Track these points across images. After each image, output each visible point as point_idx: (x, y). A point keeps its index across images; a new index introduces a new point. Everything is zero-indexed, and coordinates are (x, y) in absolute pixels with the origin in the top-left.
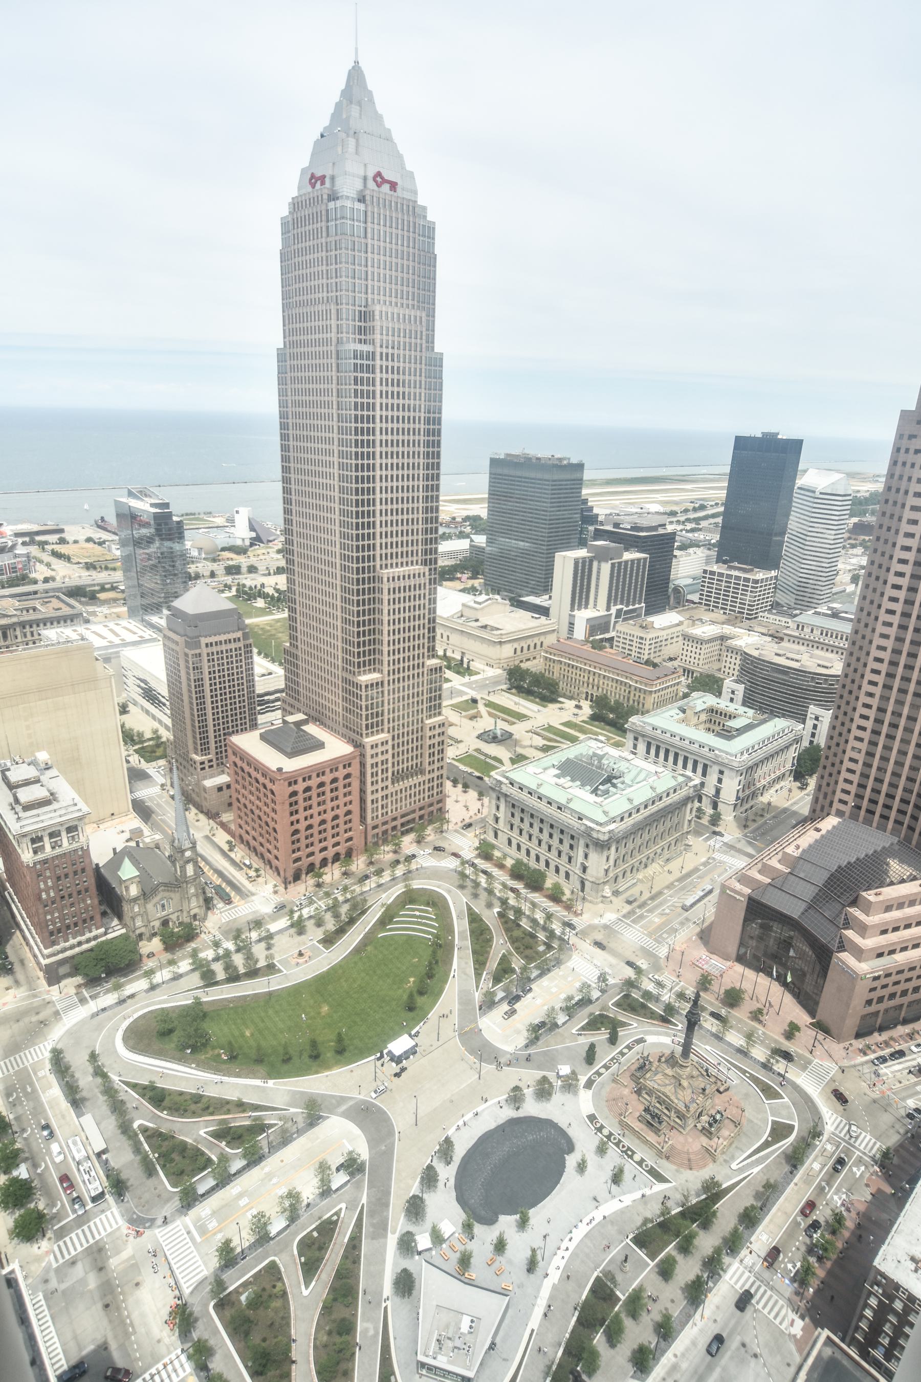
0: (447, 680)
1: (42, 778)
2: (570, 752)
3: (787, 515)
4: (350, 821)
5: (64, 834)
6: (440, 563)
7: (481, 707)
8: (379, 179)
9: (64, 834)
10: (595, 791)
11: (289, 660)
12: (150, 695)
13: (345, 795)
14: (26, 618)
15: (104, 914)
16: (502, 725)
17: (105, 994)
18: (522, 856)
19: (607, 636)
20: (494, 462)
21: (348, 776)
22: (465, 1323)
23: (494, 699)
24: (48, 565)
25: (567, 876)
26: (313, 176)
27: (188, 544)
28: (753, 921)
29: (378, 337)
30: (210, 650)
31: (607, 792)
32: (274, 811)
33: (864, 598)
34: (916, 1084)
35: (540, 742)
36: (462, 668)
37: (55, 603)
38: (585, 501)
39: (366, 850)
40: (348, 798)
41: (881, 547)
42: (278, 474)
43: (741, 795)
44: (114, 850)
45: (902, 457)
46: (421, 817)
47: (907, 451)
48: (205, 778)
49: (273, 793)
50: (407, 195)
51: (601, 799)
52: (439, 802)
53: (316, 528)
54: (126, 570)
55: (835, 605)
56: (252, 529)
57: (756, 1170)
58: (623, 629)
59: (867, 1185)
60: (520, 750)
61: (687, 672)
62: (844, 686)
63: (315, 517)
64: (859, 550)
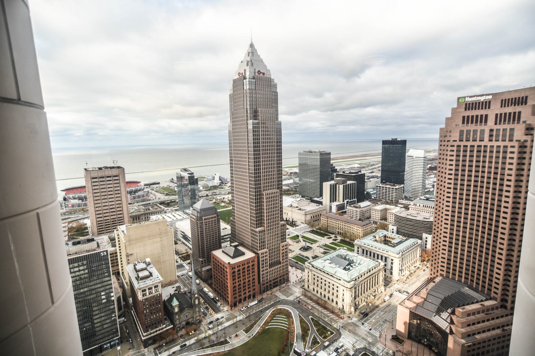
0: (288, 229)
1: (148, 268)
2: (334, 254)
3: (404, 165)
5: (153, 288)
6: (284, 188)
7: (300, 238)
9: (153, 288)
10: (345, 269)
11: (233, 224)
12: (185, 237)
13: (252, 272)
14: (146, 212)
16: (308, 244)
17: (165, 351)
18: (319, 295)
19: (344, 211)
20: (300, 154)
21: (253, 265)
24: (154, 195)
25: (337, 303)
27: (199, 186)
29: (260, 118)
31: (349, 269)
32: (227, 279)
33: (438, 193)
35: (322, 250)
36: (293, 224)
37: (156, 207)
38: (332, 165)
39: (261, 294)
41: (441, 174)
42: (229, 162)
46: (280, 280)
48: (203, 267)
49: (227, 272)
50: (268, 76)
54: (179, 196)
55: (427, 196)
56: (220, 180)
58: (349, 208)
61: (375, 223)
62: (435, 225)
63: (241, 175)
64: (433, 176)
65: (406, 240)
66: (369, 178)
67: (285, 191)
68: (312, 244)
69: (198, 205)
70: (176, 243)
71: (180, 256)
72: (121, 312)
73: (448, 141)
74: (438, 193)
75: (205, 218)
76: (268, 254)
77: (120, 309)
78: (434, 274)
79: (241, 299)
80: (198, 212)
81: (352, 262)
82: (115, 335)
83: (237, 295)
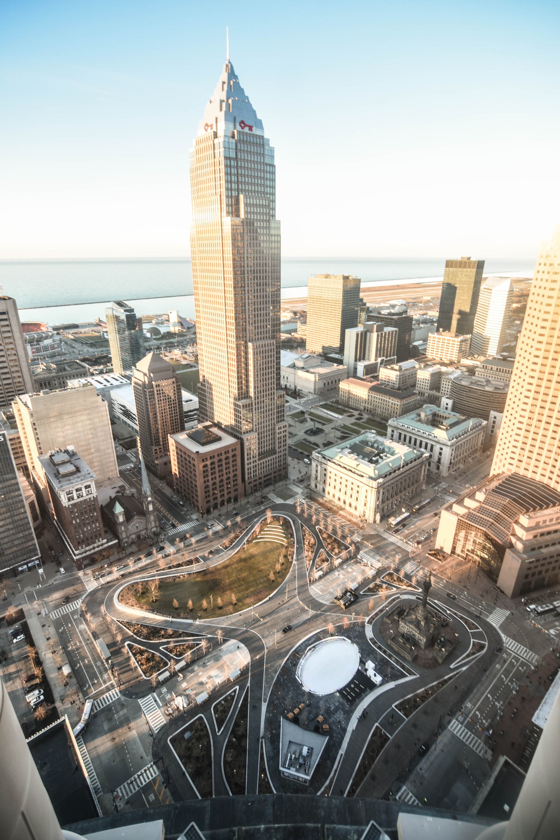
0: (287, 402)
2: (357, 440)
4: (236, 480)
5: (83, 489)
7: (306, 416)
8: (243, 125)
9: (83, 489)
10: (371, 461)
12: (127, 413)
15: (106, 532)
19: (375, 374)
21: (234, 456)
22: (305, 751)
23: (313, 411)
25: (356, 508)
30: (158, 388)
32: (195, 475)
34: (555, 621)
35: (339, 434)
37: (76, 366)
38: (362, 300)
40: (235, 468)
43: (452, 461)
44: (110, 497)
46: (275, 477)
49: (194, 465)
51: (374, 465)
52: (285, 468)
53: (213, 320)
55: (505, 354)
57: (464, 669)
59: (528, 677)
60: (328, 439)
61: (421, 394)
65: (465, 420)
66: (418, 322)
67: (284, 342)
68: (324, 424)
69: (144, 364)
70: (113, 423)
71: (121, 442)
72: (38, 522)
73: (551, 265)
77: (35, 518)
78: (499, 468)
79: (216, 504)
82: (32, 554)
83: (211, 498)
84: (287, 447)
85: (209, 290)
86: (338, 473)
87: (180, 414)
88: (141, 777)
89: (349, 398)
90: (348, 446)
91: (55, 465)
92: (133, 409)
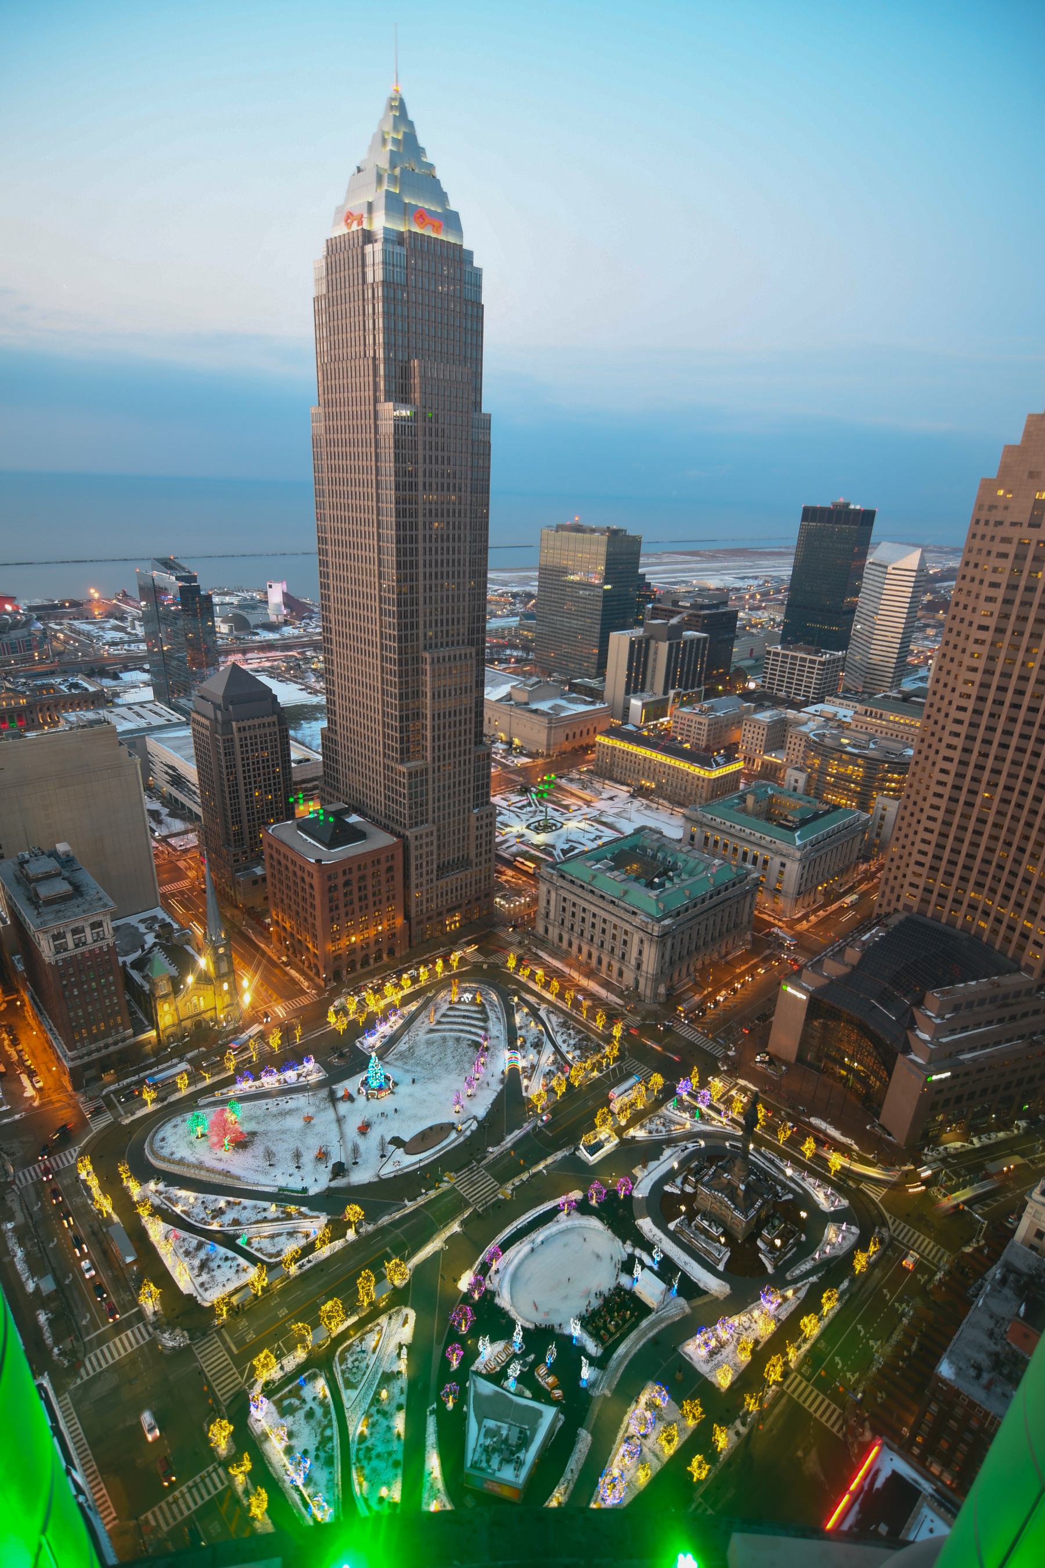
5: (88, 930)
9: (88, 930)
10: (651, 885)
12: (178, 780)
21: (390, 869)
25: (621, 973)
26: (349, 216)
28: (816, 1019)
30: (242, 735)
31: (662, 885)
32: (313, 906)
33: (938, 681)
41: (956, 625)
42: (314, 546)
45: (981, 530)
47: (987, 523)
48: (238, 871)
49: (311, 886)
51: (657, 892)
52: (487, 895)
63: (354, 593)
74: (938, 681)
75: (242, 724)
76: (434, 838)
78: (889, 904)
80: (217, 707)
81: (674, 869)
84: (492, 856)
85: (347, 544)
86: (586, 905)
87: (286, 787)
88: (194, 1490)
89: (612, 764)
90: (609, 856)
91: (30, 880)
92: (190, 771)
